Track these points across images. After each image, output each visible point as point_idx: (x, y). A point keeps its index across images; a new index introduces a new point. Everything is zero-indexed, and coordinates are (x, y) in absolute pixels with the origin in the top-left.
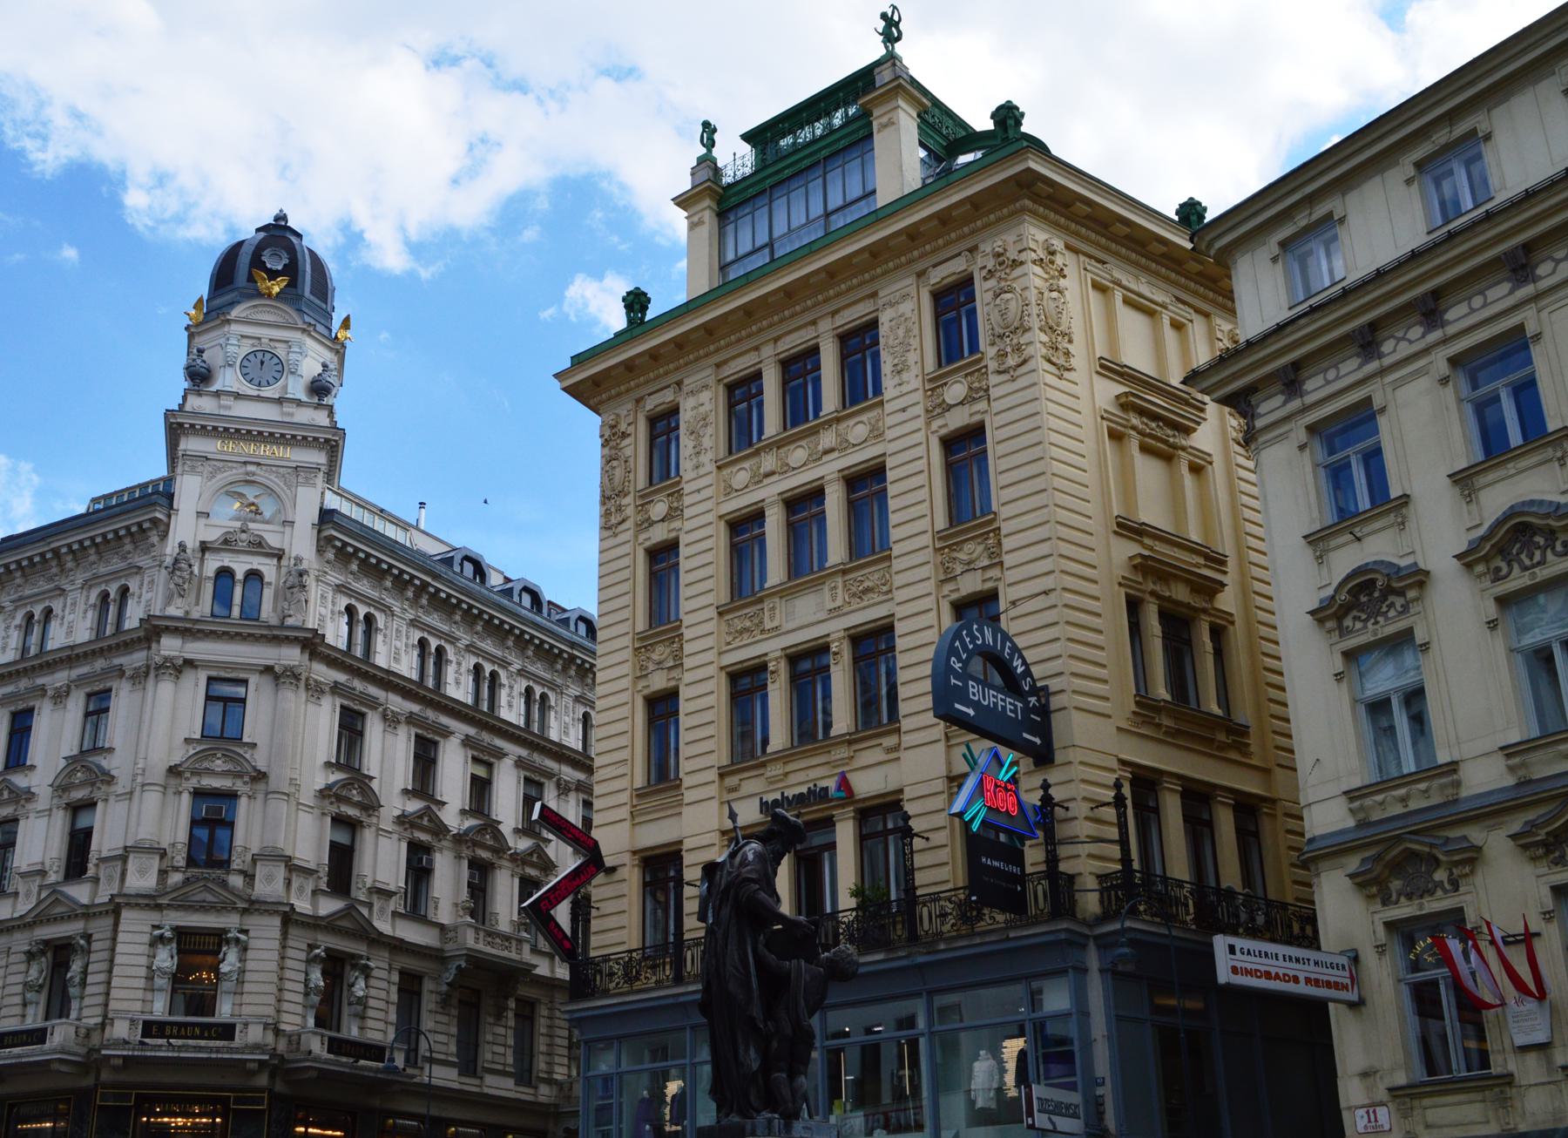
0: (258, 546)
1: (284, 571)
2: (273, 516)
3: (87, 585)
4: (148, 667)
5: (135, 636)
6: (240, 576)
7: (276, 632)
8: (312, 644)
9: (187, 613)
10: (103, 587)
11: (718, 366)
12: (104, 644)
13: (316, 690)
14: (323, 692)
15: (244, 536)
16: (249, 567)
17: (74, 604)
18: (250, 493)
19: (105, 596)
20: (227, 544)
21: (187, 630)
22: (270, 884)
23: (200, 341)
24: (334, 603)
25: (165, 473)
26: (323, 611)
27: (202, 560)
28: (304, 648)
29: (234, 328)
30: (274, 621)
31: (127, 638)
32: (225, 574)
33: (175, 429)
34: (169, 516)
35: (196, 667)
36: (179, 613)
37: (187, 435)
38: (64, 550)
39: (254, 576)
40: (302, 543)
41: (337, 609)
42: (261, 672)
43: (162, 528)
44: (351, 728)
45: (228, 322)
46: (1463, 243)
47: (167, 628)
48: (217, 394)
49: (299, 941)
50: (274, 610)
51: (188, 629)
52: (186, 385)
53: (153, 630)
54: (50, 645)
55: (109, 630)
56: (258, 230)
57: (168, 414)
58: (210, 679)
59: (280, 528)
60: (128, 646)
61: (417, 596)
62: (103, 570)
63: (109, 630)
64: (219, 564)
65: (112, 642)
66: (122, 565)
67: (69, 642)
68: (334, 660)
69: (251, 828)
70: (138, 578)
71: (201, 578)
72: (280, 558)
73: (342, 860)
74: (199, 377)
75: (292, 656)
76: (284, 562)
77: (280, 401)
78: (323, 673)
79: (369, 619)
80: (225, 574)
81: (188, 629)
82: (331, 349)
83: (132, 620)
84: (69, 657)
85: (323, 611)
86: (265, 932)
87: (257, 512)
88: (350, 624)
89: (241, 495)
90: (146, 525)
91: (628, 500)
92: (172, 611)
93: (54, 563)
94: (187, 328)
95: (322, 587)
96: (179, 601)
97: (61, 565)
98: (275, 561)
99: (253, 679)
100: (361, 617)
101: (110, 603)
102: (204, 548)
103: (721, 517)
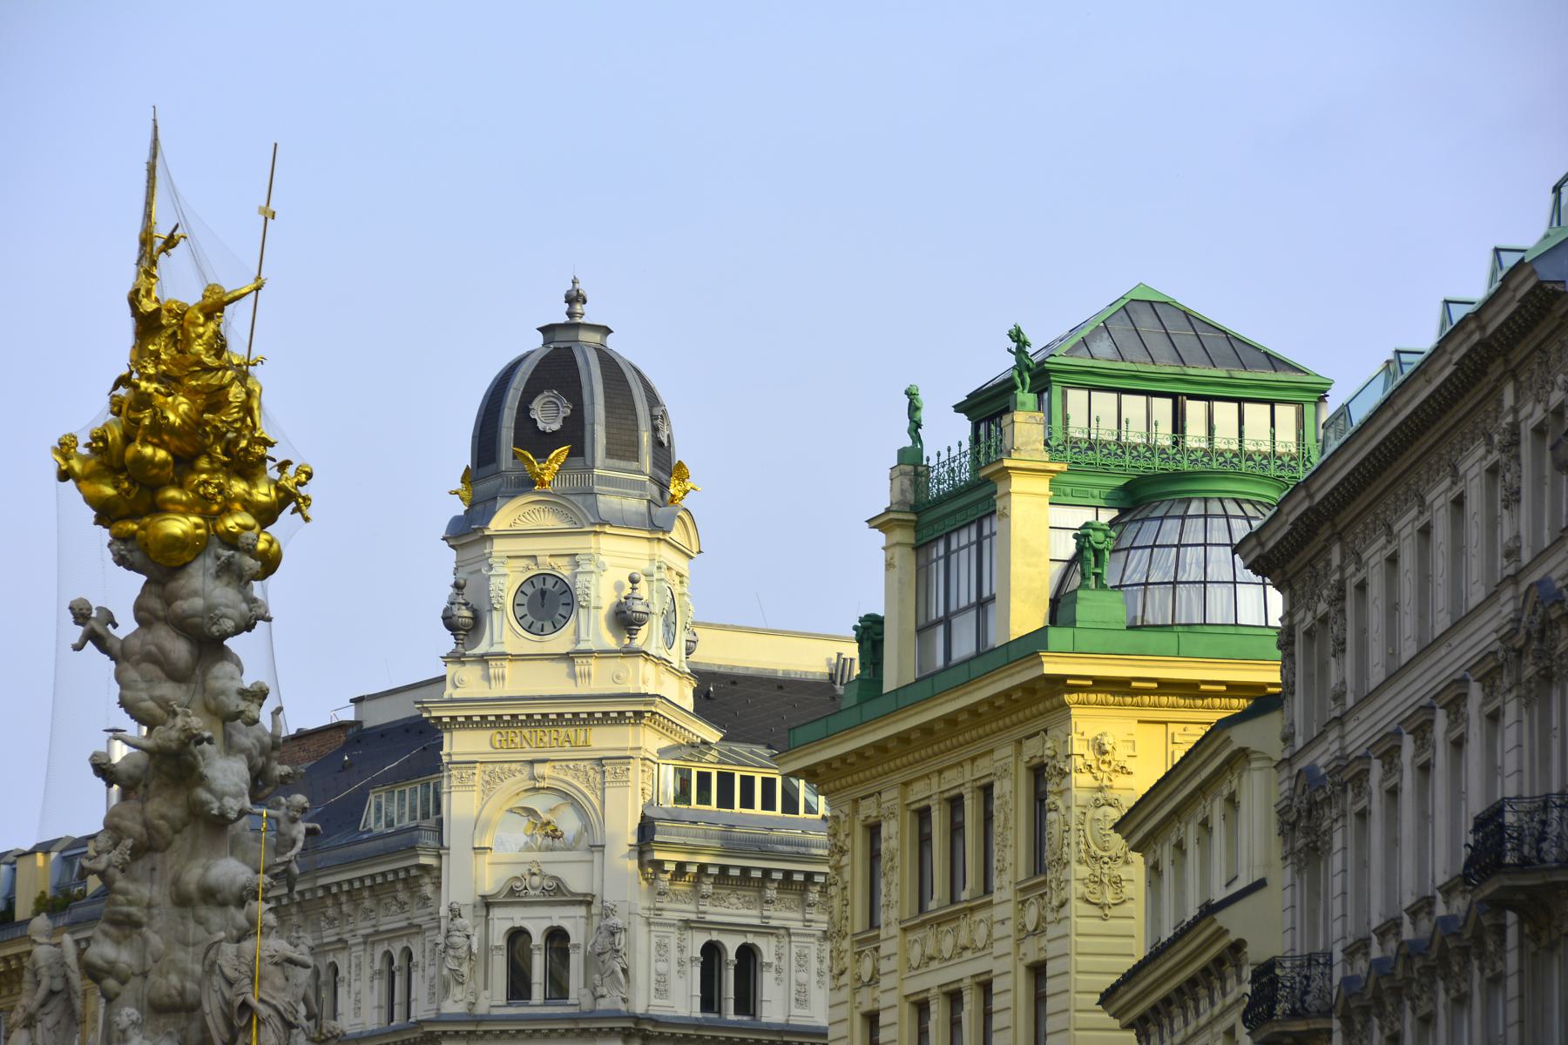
0: (557, 894)
2: (578, 838)
3: (369, 941)
6: (538, 939)
11: (906, 784)
15: (536, 880)
16: (547, 924)
17: (359, 966)
18: (539, 803)
20: (513, 895)
24: (681, 949)
29: (499, 547)
32: (517, 936)
34: (440, 857)
36: (460, 1008)
37: (450, 731)
39: (557, 937)
43: (435, 873)
45: (491, 538)
46: (1145, 977)
48: (483, 659)
59: (587, 857)
64: (508, 925)
71: (487, 949)
72: (589, 904)
76: (595, 910)
77: (568, 657)
79: (748, 955)
80: (517, 936)
87: (555, 835)
89: (530, 812)
90: (413, 872)
91: (846, 944)
96: (457, 992)
98: (582, 911)
102: (487, 903)
103: (906, 997)
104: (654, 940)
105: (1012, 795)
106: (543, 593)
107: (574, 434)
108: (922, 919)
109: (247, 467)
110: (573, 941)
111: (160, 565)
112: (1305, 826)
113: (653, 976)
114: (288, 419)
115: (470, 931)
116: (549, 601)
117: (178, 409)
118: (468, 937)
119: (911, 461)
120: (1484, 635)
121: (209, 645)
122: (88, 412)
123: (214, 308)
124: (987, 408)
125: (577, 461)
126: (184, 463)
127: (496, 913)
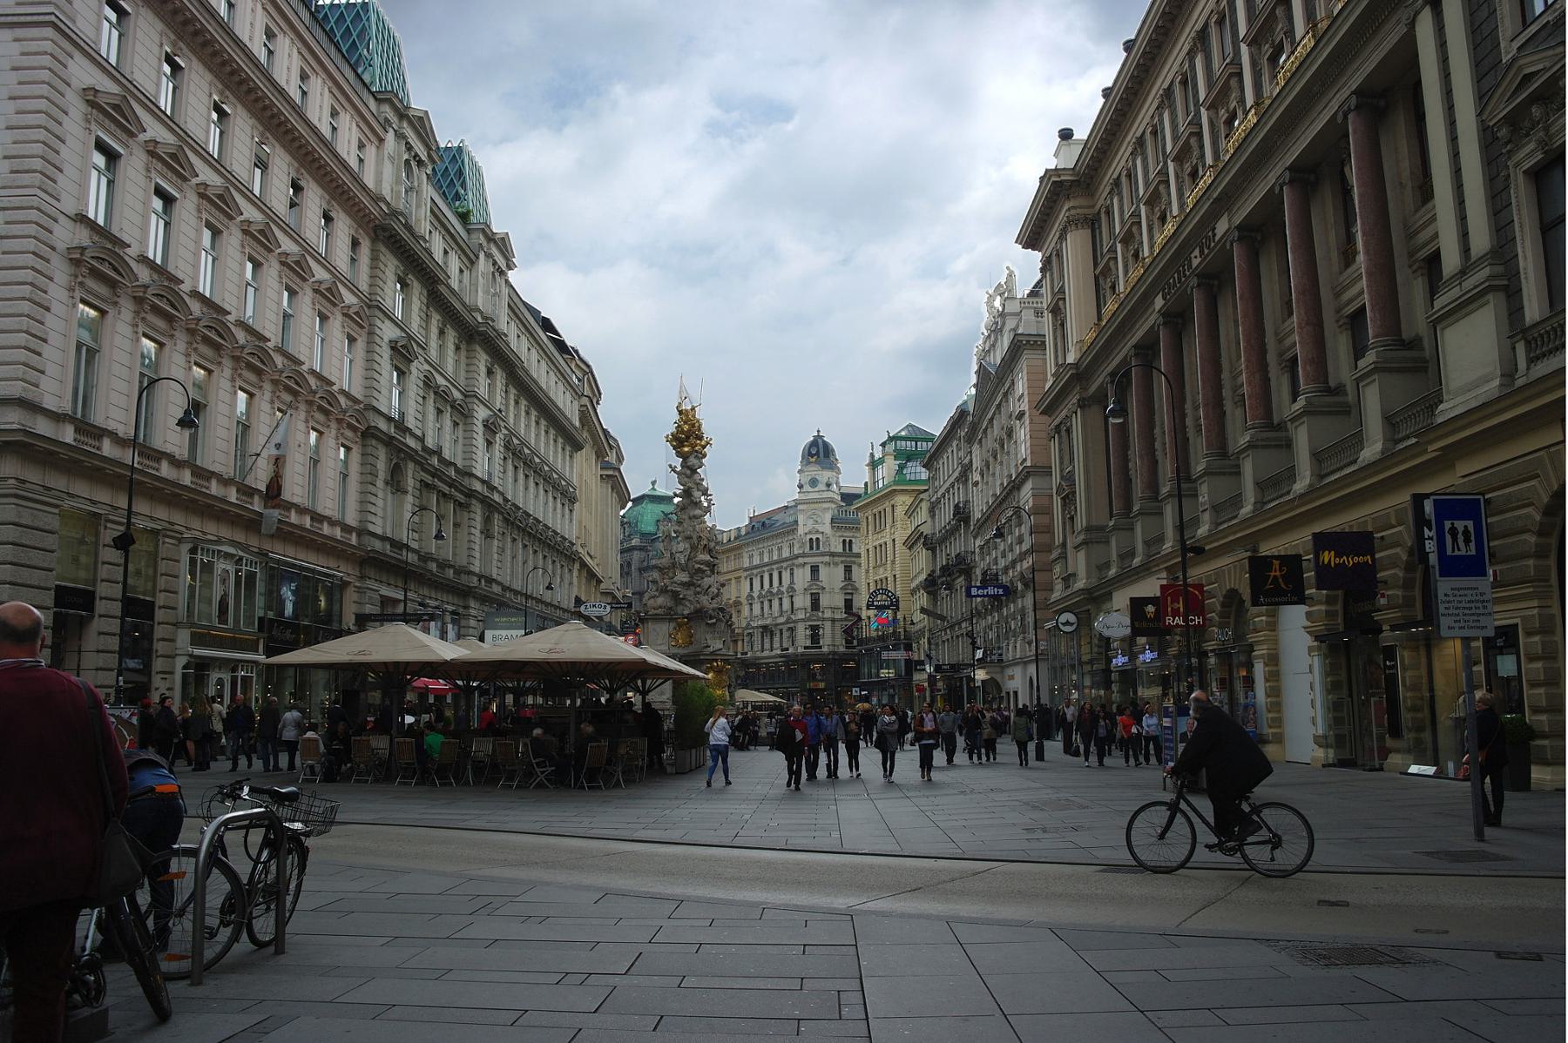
8: (832, 555)
13: (836, 564)
22: (828, 614)
40: (827, 528)
44: (848, 570)
49: (838, 624)
51: (804, 555)
53: (797, 557)
68: (839, 555)
69: (824, 601)
73: (848, 604)
75: (827, 559)
78: (837, 559)
81: (804, 555)
86: (828, 625)
101: (791, 546)
105: (889, 510)
107: (817, 454)
108: (875, 532)
109: (701, 438)
111: (684, 457)
112: (932, 511)
114: (707, 430)
117: (686, 427)
119: (872, 455)
120: (956, 474)
121: (694, 471)
122: (672, 429)
123: (693, 409)
124: (883, 445)
126: (688, 438)
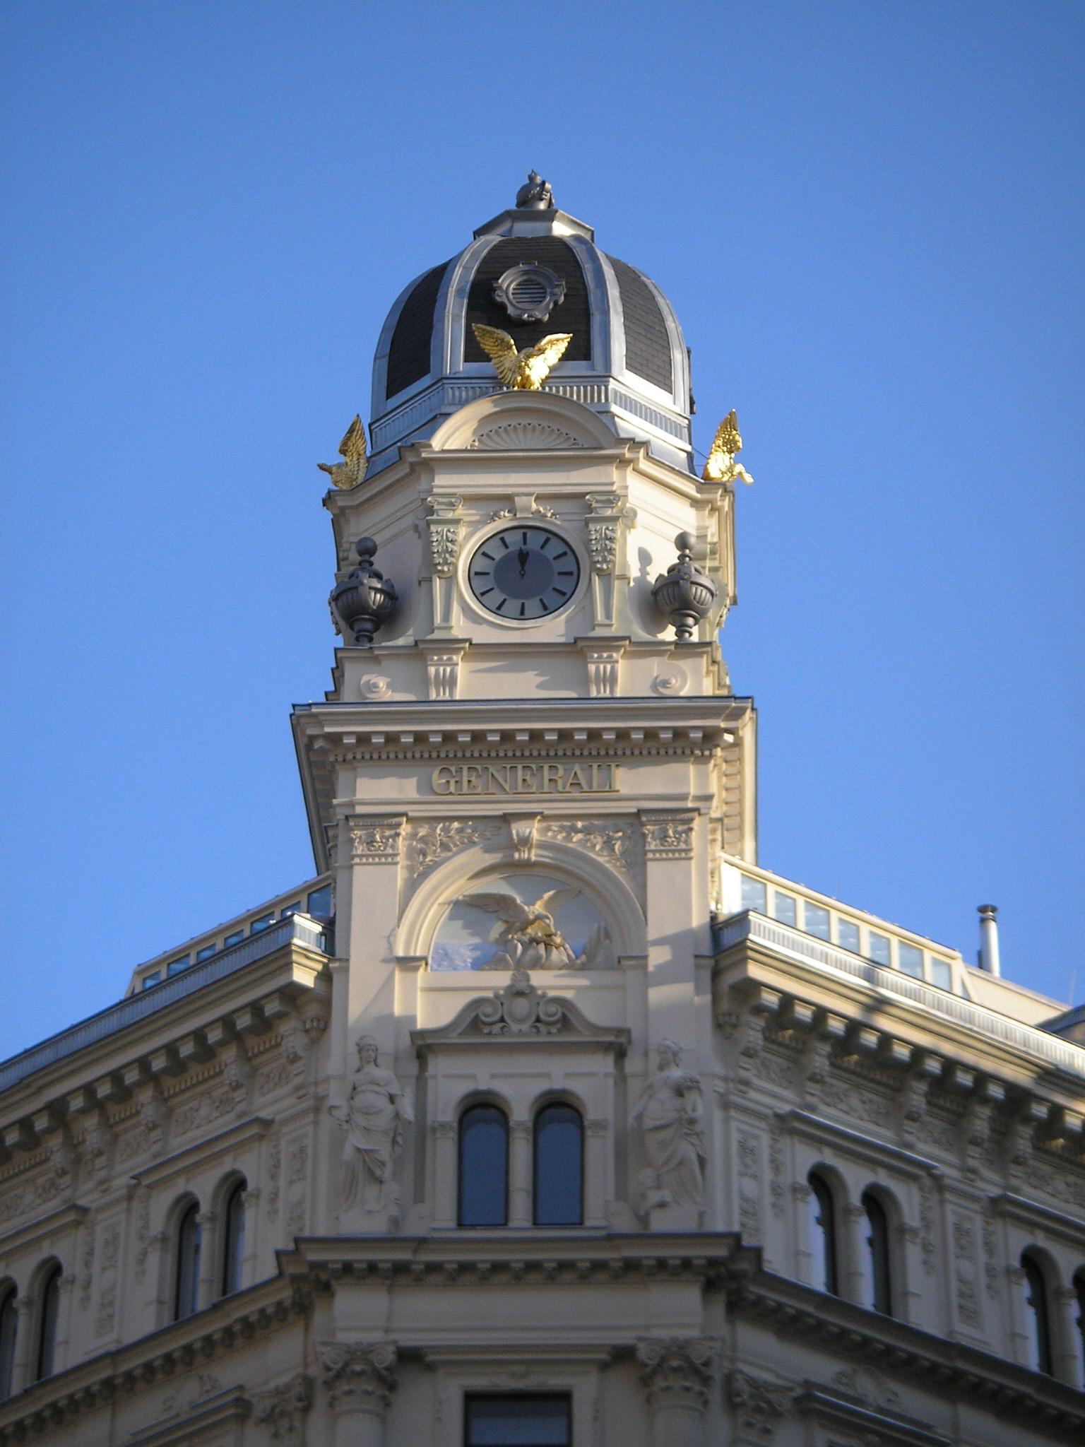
1: (634, 1086)
4: (308, 1382)
5: (267, 1302)
6: (521, 1113)
7: (629, 1252)
9: (395, 1222)
10: (180, 1187)
12: (193, 1336)
14: (776, 1414)
15: (521, 1006)
17: (112, 1242)
19: (187, 1210)
21: (400, 1269)
23: (358, 528)
25: (307, 872)
26: (749, 1187)
27: (421, 1080)
28: (710, 1287)
29: (444, 481)
30: (624, 1224)
31: (249, 1309)
33: (323, 756)
35: (431, 1367)
36: (378, 1226)
38: (77, 1103)
41: (786, 1180)
42: (604, 1366)
43: (313, 1010)
45: (431, 465)
47: (347, 1268)
50: (621, 1194)
52: (339, 642)
54: (61, 1362)
55: (203, 1298)
56: (478, 233)
57: (300, 717)
58: (472, 1399)
60: (251, 1331)
61: (1002, 1133)
62: (179, 1142)
63: (203, 1298)
64: (464, 1088)
65: (214, 1327)
66: (226, 1121)
67: (107, 1342)
70: (265, 1147)
74: (370, 613)
75: (677, 1313)
76: (633, 1064)
81: (400, 1267)
82: (695, 503)
83: (256, 1265)
84: (108, 1384)
85: (749, 1187)
88: (829, 1221)
92: (356, 1223)
93: (55, 1142)
94: (328, 501)
95: (738, 1123)
97: (72, 1144)
99: (584, 1389)
100: (855, 1199)
104: (735, 1137)
106: (523, 557)
110: (591, 1115)
113: (736, 1202)
115: (395, 1089)
116: (537, 568)
118: (392, 1099)
125: (579, 368)
127: (439, 1066)
